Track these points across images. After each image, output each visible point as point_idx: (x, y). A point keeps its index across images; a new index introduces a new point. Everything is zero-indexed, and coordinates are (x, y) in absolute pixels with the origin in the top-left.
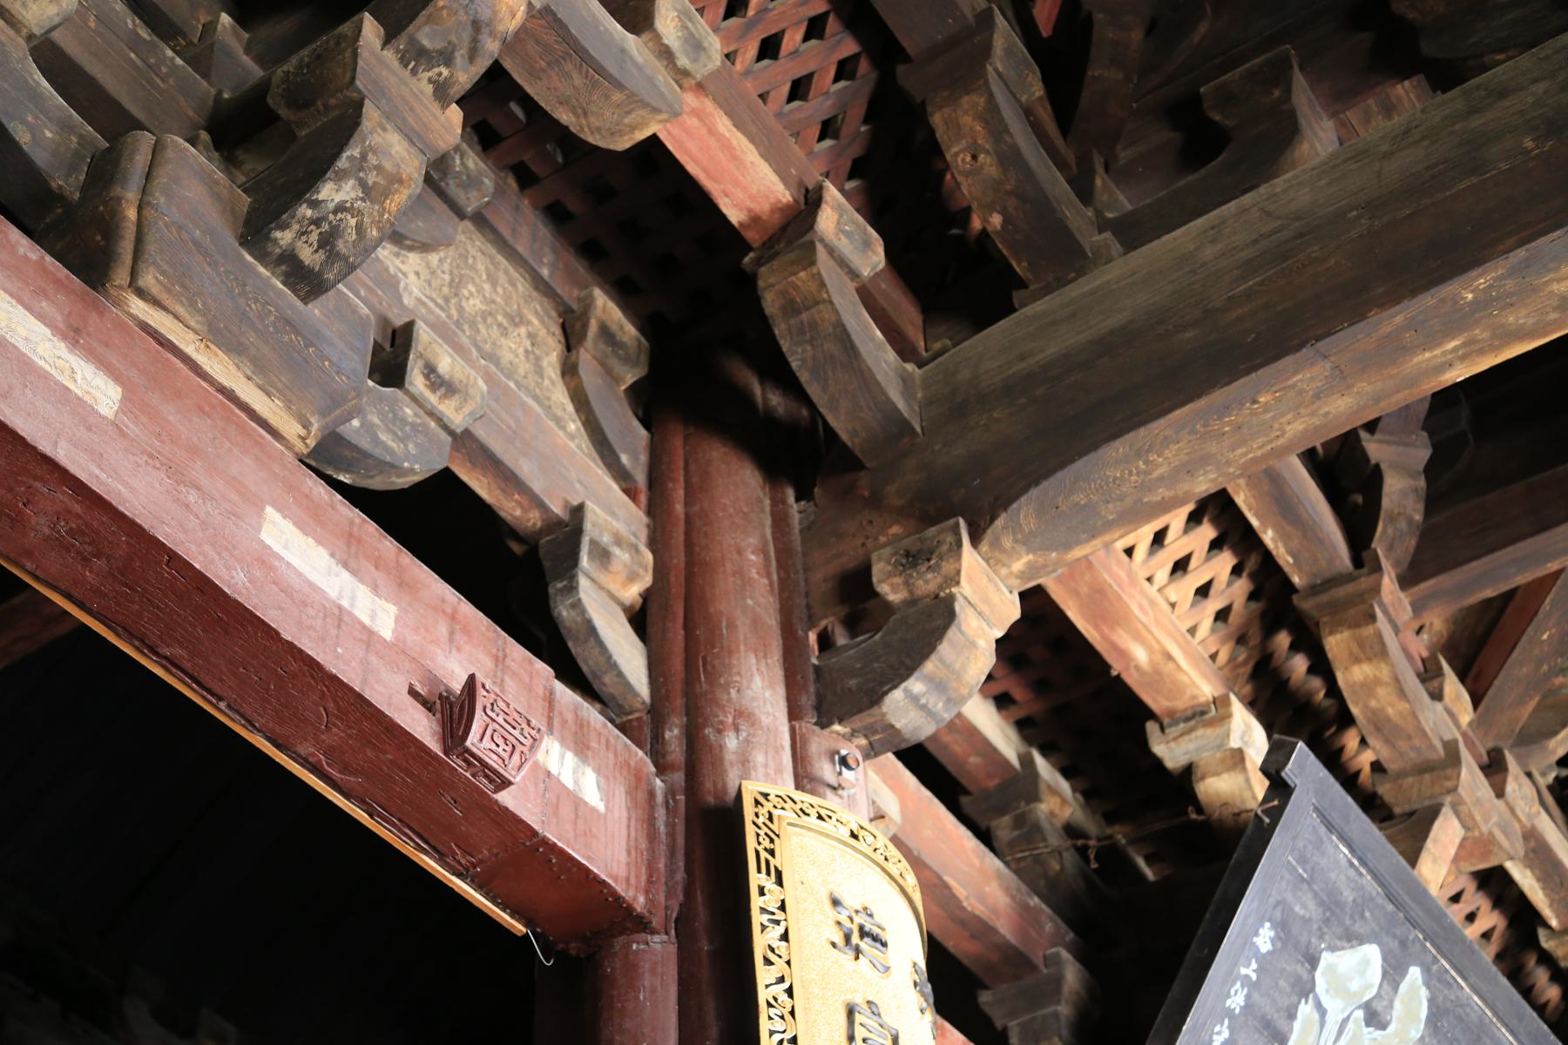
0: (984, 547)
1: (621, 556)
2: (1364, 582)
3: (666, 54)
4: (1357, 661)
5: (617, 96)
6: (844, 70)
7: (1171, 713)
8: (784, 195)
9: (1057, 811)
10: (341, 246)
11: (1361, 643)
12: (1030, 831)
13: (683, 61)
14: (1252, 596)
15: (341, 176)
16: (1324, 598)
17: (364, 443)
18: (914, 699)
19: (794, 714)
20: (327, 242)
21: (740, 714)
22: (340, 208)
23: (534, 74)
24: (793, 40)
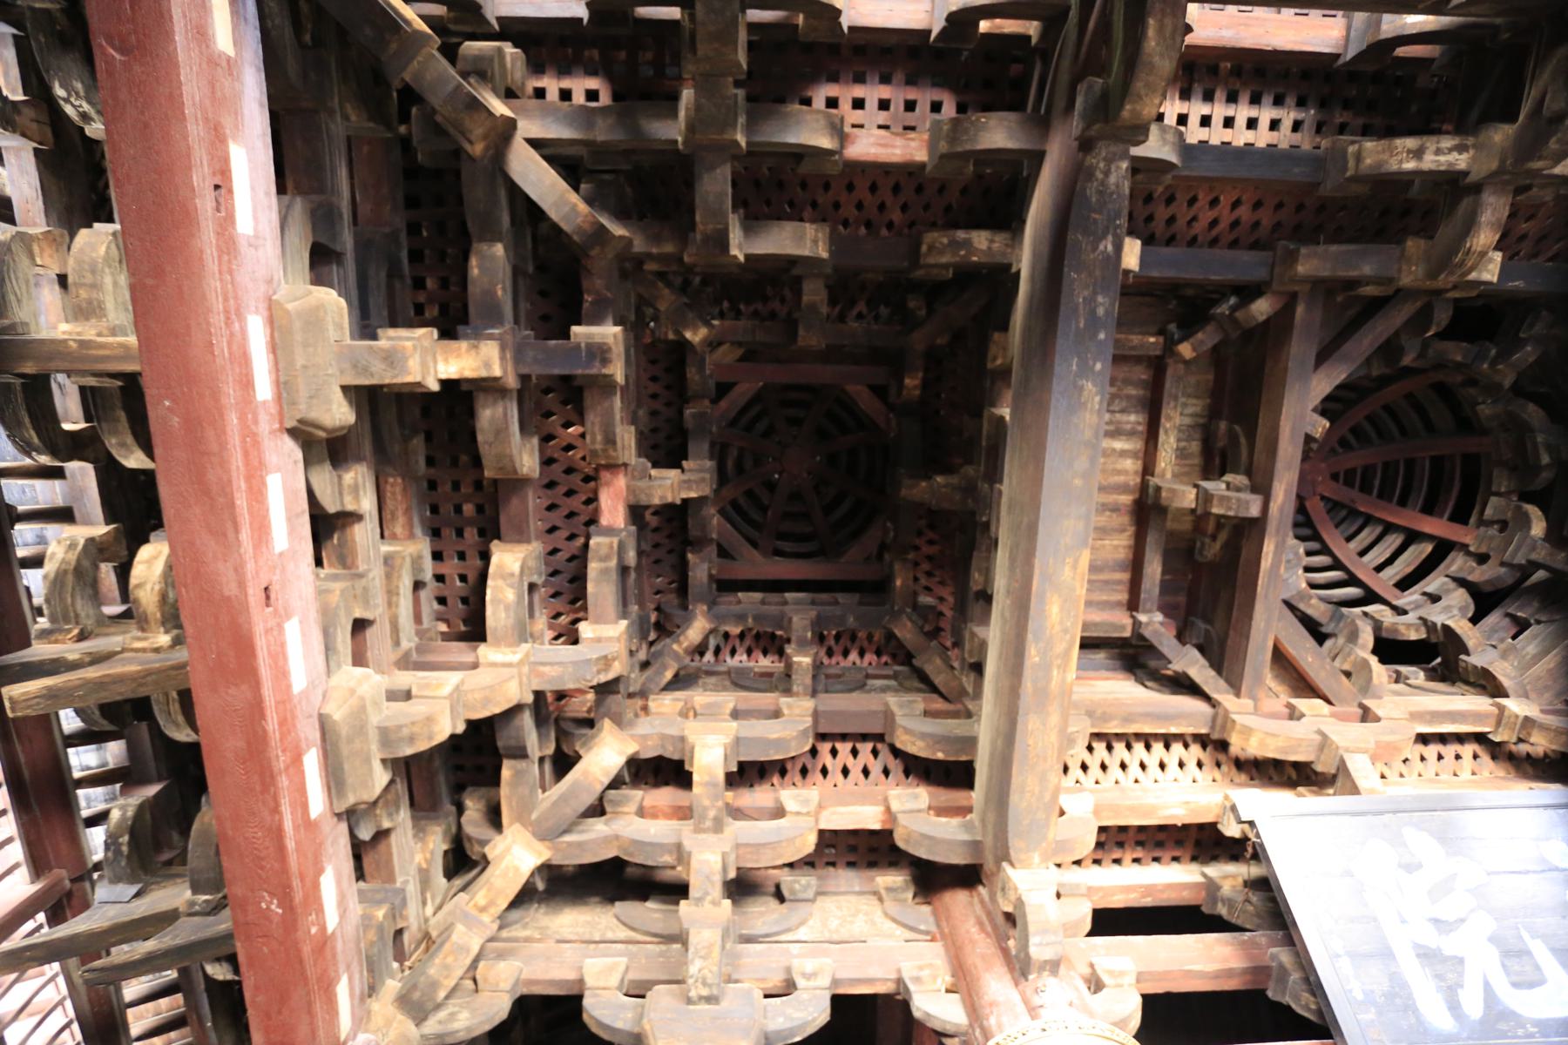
0: (1017, 865)
1: (925, 973)
2: (1221, 711)
3: (798, 813)
4: (1247, 740)
5: (784, 844)
6: (875, 753)
7: (1218, 816)
8: (881, 809)
9: (1234, 883)
10: (709, 981)
11: (1241, 732)
12: (1230, 903)
13: (804, 810)
14: (1204, 747)
15: (693, 961)
16: (1218, 728)
17: (788, 1025)
18: (1036, 945)
19: (1017, 984)
20: (705, 984)
21: (991, 1005)
22: (700, 971)
23: (757, 861)
24: (850, 761)
